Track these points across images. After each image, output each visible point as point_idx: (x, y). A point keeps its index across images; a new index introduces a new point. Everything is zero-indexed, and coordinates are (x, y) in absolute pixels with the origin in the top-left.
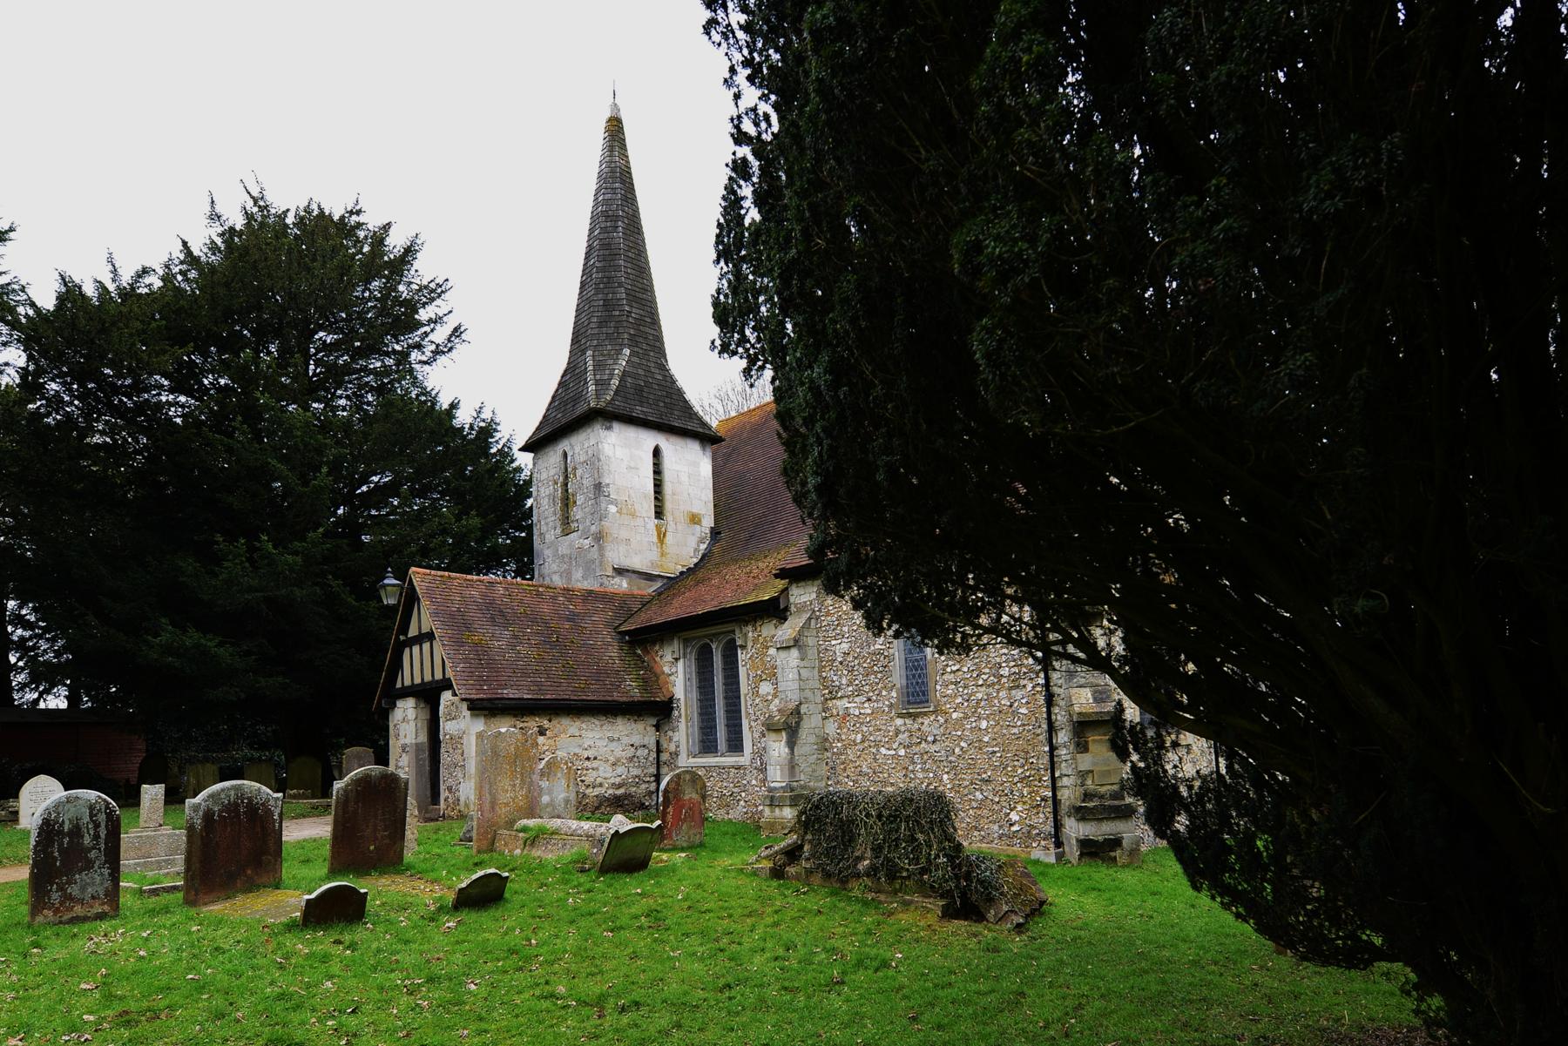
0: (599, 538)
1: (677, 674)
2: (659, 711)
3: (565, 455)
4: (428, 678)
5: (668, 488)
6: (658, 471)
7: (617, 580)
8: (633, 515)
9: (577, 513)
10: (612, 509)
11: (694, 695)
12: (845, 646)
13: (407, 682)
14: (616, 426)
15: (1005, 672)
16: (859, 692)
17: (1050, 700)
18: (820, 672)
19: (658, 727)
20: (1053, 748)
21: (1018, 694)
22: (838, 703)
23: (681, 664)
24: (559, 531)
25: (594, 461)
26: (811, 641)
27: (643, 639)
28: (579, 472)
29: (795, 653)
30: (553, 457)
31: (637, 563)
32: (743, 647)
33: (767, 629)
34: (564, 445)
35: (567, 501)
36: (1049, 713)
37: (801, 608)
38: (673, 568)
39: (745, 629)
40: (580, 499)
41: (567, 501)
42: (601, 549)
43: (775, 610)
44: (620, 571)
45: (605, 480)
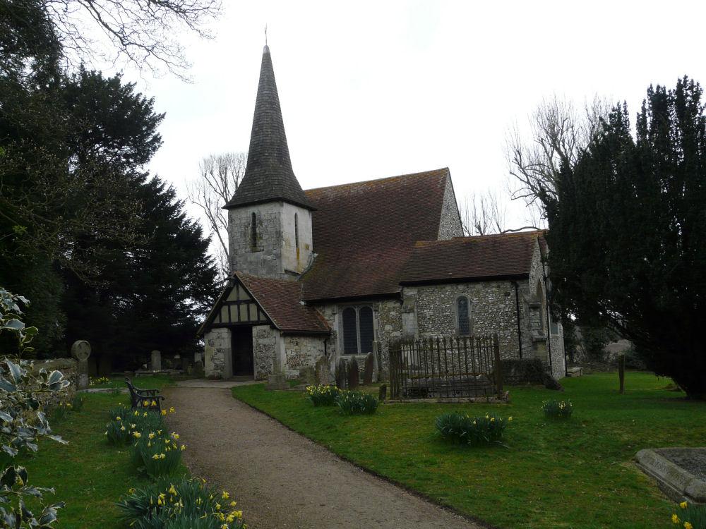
0: (279, 256)
1: (334, 320)
2: (325, 336)
3: (254, 215)
4: (244, 318)
5: (300, 233)
6: (296, 225)
7: (286, 276)
8: (290, 245)
9: (259, 242)
10: (284, 243)
11: (342, 329)
12: (431, 313)
13: (225, 319)
14: (285, 204)
15: (502, 324)
16: (438, 329)
17: (520, 334)
18: (419, 321)
19: (325, 342)
20: (521, 349)
21: (507, 332)
22: (426, 334)
23: (336, 317)
24: (249, 249)
25: (276, 221)
26: (416, 310)
27: (314, 304)
28: (265, 224)
29: (412, 314)
30: (245, 214)
31: (291, 268)
32: (376, 311)
33: (391, 304)
34: (254, 209)
35: (255, 236)
36: (520, 338)
37: (410, 298)
38: (301, 270)
39: (377, 304)
40: (265, 237)
41: (255, 236)
42: (281, 262)
43: (398, 297)
44: (287, 271)
45: (282, 230)
